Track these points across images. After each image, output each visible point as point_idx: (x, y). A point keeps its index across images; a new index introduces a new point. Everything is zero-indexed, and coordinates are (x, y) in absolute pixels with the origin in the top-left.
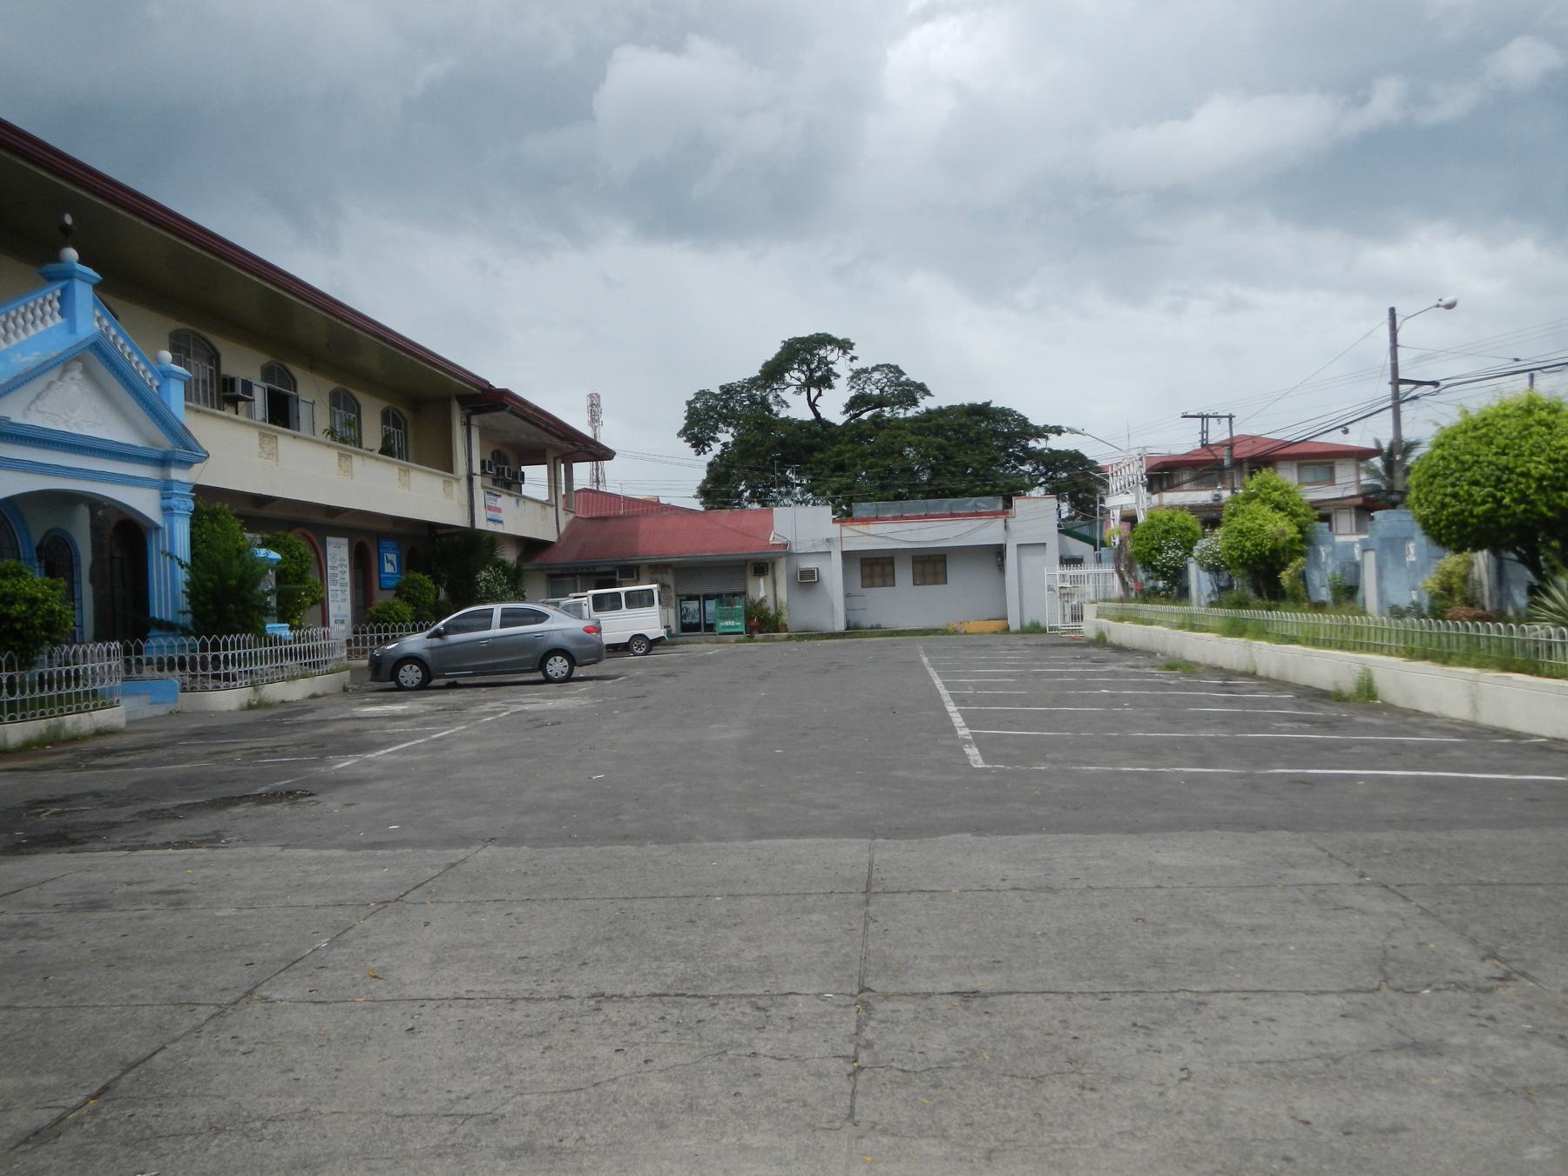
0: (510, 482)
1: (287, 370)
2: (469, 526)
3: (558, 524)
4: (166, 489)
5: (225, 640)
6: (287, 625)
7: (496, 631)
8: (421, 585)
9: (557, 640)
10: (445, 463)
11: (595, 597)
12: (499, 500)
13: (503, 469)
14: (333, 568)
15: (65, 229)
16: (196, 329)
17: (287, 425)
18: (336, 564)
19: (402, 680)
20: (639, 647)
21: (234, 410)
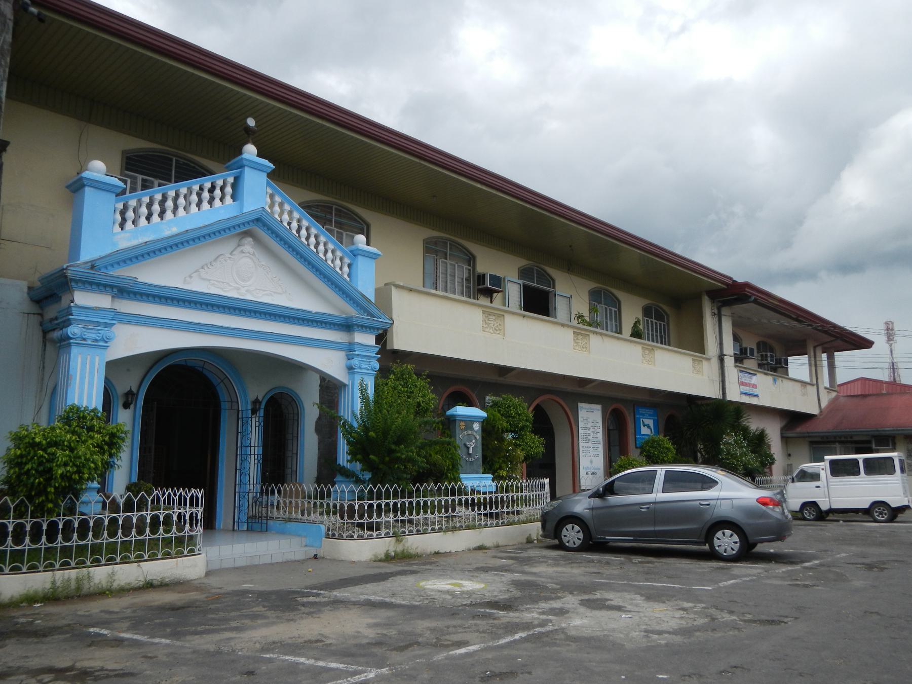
0: (777, 368)
1: (545, 272)
2: (720, 397)
3: (819, 400)
4: (350, 349)
5: (387, 490)
6: (490, 476)
7: (658, 495)
8: (660, 445)
9: (724, 510)
10: (698, 346)
11: (832, 463)
12: (754, 378)
13: (766, 355)
14: (585, 428)
15: (248, 129)
16: (453, 238)
17: (548, 315)
18: (589, 426)
19: (565, 540)
20: (881, 513)
21: (489, 299)
